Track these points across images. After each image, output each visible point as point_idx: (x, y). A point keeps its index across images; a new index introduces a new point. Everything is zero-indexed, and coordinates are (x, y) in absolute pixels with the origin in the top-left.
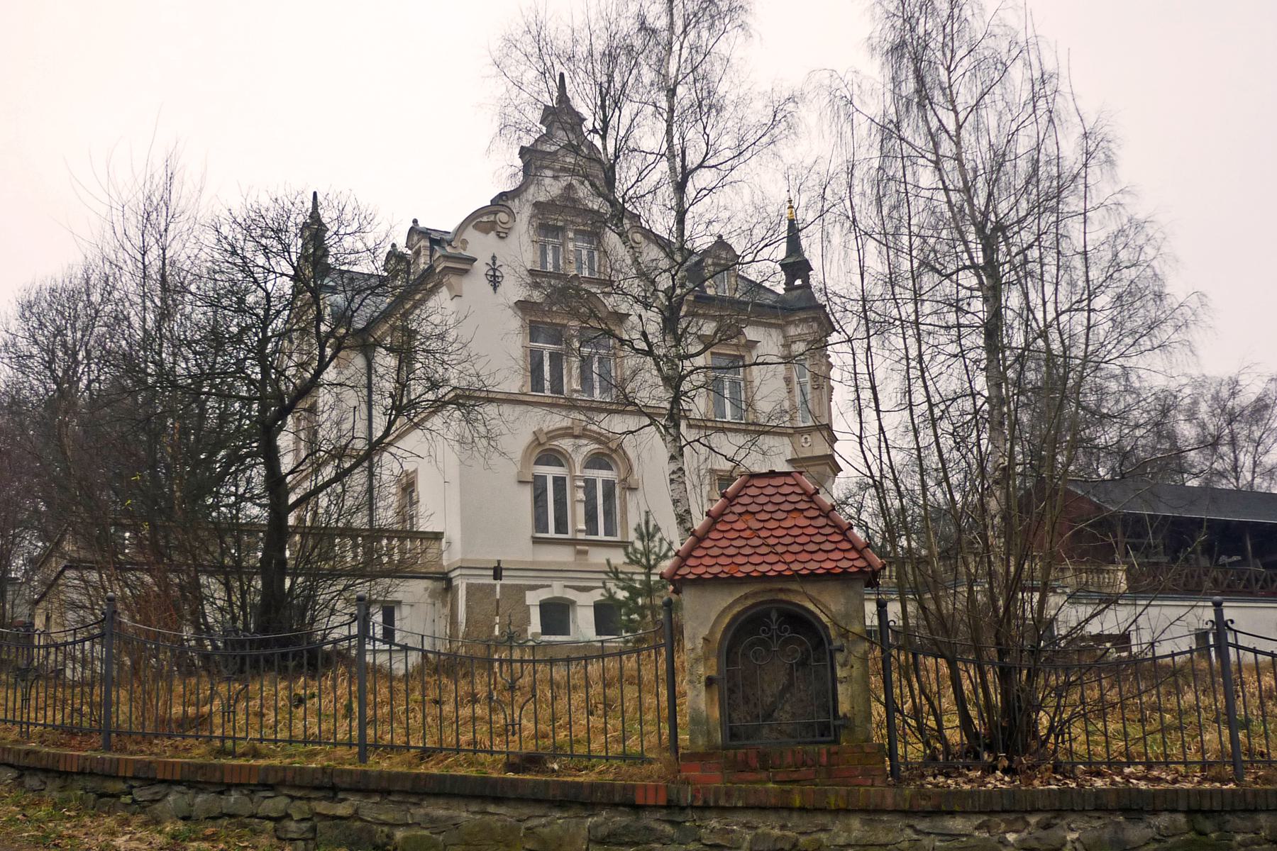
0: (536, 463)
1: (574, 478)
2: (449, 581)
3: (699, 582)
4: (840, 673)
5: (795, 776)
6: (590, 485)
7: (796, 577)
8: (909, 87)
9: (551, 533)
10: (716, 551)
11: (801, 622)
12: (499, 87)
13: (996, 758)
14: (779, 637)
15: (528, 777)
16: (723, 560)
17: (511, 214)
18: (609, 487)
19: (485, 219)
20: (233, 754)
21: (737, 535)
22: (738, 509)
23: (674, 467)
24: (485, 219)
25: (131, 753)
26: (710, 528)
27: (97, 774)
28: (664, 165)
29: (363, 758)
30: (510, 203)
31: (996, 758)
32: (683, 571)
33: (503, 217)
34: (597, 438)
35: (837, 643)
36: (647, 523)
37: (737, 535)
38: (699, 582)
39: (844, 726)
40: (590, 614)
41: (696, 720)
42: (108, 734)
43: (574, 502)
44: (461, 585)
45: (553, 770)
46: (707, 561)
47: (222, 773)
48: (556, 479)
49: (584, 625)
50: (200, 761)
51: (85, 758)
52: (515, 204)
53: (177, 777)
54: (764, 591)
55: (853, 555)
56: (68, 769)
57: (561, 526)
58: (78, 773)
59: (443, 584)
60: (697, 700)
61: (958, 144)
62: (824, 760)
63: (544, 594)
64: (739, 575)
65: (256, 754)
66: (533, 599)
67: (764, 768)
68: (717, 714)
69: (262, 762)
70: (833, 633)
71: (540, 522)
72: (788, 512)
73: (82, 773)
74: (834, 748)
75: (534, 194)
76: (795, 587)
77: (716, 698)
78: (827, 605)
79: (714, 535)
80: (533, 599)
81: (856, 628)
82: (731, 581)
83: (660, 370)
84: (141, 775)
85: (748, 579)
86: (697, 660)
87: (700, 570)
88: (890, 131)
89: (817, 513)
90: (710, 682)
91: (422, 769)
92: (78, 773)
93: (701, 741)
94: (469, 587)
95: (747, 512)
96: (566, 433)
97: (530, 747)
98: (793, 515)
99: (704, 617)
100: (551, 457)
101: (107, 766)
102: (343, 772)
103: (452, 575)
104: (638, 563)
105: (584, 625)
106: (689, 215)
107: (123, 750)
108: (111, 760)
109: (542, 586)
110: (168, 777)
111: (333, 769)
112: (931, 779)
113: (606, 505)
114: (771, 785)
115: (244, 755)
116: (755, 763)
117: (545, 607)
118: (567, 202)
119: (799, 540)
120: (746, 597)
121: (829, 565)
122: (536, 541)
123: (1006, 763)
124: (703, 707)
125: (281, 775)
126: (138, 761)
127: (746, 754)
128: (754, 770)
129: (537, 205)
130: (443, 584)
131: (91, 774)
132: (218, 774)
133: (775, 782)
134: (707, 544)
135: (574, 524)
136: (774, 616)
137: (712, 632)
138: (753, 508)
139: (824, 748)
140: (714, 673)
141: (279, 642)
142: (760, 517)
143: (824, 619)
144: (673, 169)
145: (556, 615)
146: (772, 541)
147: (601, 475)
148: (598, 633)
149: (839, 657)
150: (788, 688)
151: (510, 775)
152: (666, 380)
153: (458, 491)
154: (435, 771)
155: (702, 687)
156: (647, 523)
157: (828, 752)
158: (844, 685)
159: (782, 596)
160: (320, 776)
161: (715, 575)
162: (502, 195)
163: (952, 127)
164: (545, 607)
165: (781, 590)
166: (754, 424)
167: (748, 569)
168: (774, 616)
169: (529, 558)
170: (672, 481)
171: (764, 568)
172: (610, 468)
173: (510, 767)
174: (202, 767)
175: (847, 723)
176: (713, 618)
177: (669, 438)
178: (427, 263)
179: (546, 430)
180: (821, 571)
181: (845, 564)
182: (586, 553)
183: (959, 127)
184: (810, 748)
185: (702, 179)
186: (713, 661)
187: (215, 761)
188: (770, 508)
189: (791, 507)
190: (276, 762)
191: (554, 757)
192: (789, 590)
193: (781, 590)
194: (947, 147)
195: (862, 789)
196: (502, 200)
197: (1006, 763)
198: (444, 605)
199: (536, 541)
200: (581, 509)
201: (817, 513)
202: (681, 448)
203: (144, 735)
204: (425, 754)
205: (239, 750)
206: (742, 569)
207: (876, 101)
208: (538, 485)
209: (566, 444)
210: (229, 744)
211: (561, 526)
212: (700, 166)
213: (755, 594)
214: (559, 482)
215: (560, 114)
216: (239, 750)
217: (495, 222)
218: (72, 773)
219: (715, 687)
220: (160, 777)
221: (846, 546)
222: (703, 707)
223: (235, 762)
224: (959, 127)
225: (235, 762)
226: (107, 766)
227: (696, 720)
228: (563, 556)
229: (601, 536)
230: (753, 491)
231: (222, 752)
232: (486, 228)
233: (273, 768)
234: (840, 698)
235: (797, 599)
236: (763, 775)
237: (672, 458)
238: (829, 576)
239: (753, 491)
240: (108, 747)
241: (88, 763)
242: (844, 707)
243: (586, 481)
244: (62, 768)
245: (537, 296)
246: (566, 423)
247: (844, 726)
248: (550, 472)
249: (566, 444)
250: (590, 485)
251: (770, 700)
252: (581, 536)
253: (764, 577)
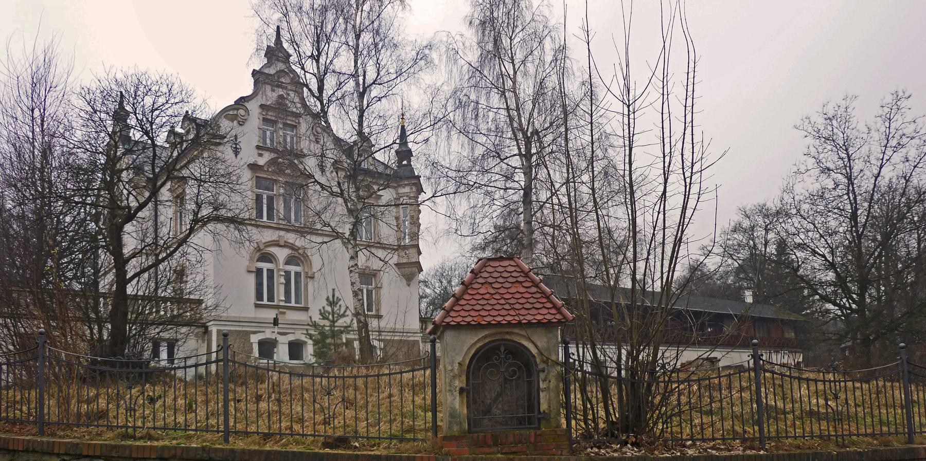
0: (257, 261)
1: (279, 270)
2: (207, 328)
3: (458, 327)
4: (542, 385)
5: (514, 450)
6: (287, 274)
7: (519, 324)
9: (265, 302)
10: (468, 308)
11: (519, 354)
13: (628, 437)
14: (505, 362)
15: (340, 452)
16: (473, 313)
17: (247, 110)
18: (298, 275)
19: (231, 113)
20: (134, 437)
21: (481, 297)
22: (481, 280)
23: (352, 263)
24: (231, 113)
25: (60, 437)
26: (464, 292)
27: (37, 452)
28: (352, 83)
29: (227, 441)
30: (246, 104)
31: (628, 437)
32: (447, 320)
33: (242, 112)
34: (292, 247)
35: (541, 366)
36: (333, 296)
37: (481, 297)
38: (458, 327)
39: (543, 418)
40: (286, 348)
41: (453, 415)
42: (42, 425)
43: (278, 284)
44: (214, 330)
45: (356, 447)
46: (463, 313)
47: (131, 450)
48: (268, 270)
49: (282, 354)
50: (112, 443)
51: (29, 441)
52: (248, 105)
53: (98, 453)
54: (496, 334)
55: (553, 311)
56: (16, 448)
57: (271, 298)
58: (23, 451)
59: (202, 330)
60: (453, 402)
61: (514, 83)
62: (532, 439)
63: (261, 336)
64: (483, 323)
65: (151, 438)
66: (255, 339)
67: (496, 444)
68: (465, 411)
69: (155, 443)
70: (538, 360)
71: (259, 296)
72: (482, 284)
73: (26, 451)
74: (538, 432)
75: (260, 100)
76: (516, 331)
77: (465, 401)
78: (533, 344)
79: (467, 297)
80: (255, 339)
81: (554, 358)
82: (480, 327)
83: (347, 205)
84: (71, 452)
85: (489, 325)
86: (454, 377)
87: (459, 319)
89: (530, 284)
90: (462, 390)
91: (267, 448)
92: (23, 451)
93: (456, 428)
94: (218, 331)
95: (517, 281)
96: (276, 244)
97: (339, 433)
98: (516, 285)
99: (457, 351)
100: (266, 257)
101: (45, 446)
102: (217, 449)
103: (208, 324)
104: (328, 319)
105: (282, 354)
106: (366, 114)
107: (53, 435)
108: (48, 442)
109: (260, 332)
110: (91, 453)
111: (210, 448)
112: (589, 450)
113: (296, 287)
114: (499, 455)
115: (141, 438)
116: (490, 442)
117: (261, 343)
118: (280, 107)
119: (520, 301)
120: (485, 337)
121: (539, 317)
122: (257, 306)
123: (634, 440)
124: (457, 406)
125: (173, 452)
126: (68, 443)
127: (485, 436)
128: (489, 446)
129: (262, 106)
130: (202, 330)
131: (34, 451)
132: (127, 452)
133: (502, 454)
134: (462, 302)
135: (278, 296)
136: (502, 349)
137: (464, 359)
138: (491, 280)
139: (532, 432)
140: (464, 385)
142: (495, 285)
143: (534, 351)
144: (357, 84)
145: (267, 347)
146: (513, 301)
147: (293, 269)
148: (290, 359)
149: (542, 376)
150: (500, 394)
151: (327, 450)
152: (350, 211)
153: (219, 272)
154: (275, 448)
155: (457, 394)
156: (333, 296)
157: (535, 434)
158: (545, 393)
159: (508, 337)
160: (201, 453)
161: (469, 322)
162: (242, 99)
163: (511, 73)
164: (261, 343)
165: (507, 333)
166: (378, 243)
167: (488, 319)
168: (502, 349)
169: (253, 316)
170: (351, 271)
171: (499, 319)
172: (298, 265)
173: (326, 445)
174: (116, 446)
175: (545, 417)
176: (465, 349)
177: (350, 246)
178: (202, 135)
179: (263, 241)
180: (534, 321)
181: (549, 317)
182: (284, 313)
183: (515, 73)
184: (523, 432)
185: (375, 91)
186: (464, 377)
187: (123, 443)
188: (501, 280)
189: (515, 280)
190: (167, 443)
191: (356, 438)
192: (512, 333)
193: (507, 333)
194: (509, 84)
195: (556, 457)
196: (241, 101)
197: (634, 440)
198: (203, 342)
199: (257, 306)
200: (282, 288)
201: (530, 284)
202: (357, 252)
203: (68, 425)
204: (267, 437)
205: (138, 435)
206: (485, 319)
207: (473, 56)
208: (259, 272)
209: (274, 250)
210: (130, 430)
211: (271, 298)
212: (374, 83)
213: (491, 335)
214: (271, 272)
215: (275, 53)
216: (138, 435)
217: (237, 115)
218: (18, 451)
219: (465, 394)
220: (85, 453)
221: (549, 305)
222: (457, 406)
223: (138, 443)
224: (515, 73)
225: (138, 443)
226: (45, 446)
227: (453, 415)
228: (271, 314)
229: (293, 304)
230: (490, 269)
231: (126, 436)
232: (233, 118)
233: (167, 447)
234: (541, 401)
235: (517, 339)
236: (495, 449)
237: (352, 258)
238: (540, 324)
239: (490, 269)
240: (42, 433)
241: (31, 444)
242: (544, 407)
243: (285, 272)
244: (11, 448)
245: (261, 161)
246: (275, 238)
247: (543, 418)
248: (265, 266)
249: (274, 250)
250: (287, 274)
251: (489, 401)
252: (282, 304)
253: (499, 324)
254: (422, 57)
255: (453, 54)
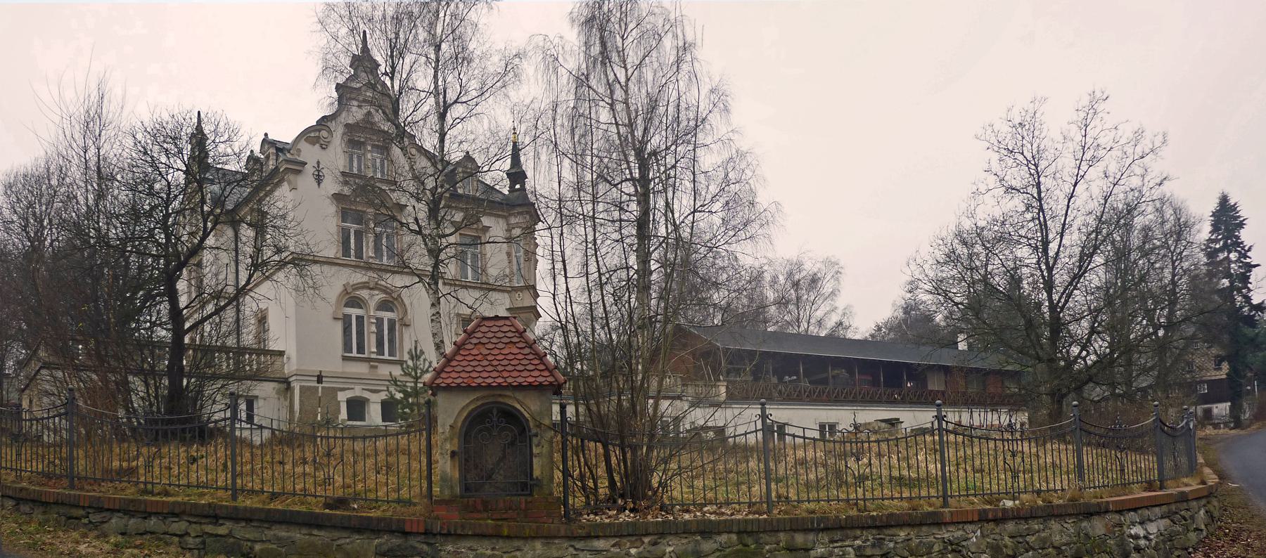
1: (369, 317)
3: (448, 388)
4: (535, 450)
6: (380, 321)
7: (510, 387)
8: (596, 50)
9: (354, 354)
11: (511, 416)
12: (323, 40)
16: (463, 375)
17: (330, 132)
18: (392, 323)
20: (152, 493)
22: (474, 341)
23: (434, 311)
26: (456, 353)
28: (432, 100)
29: (234, 498)
32: (437, 381)
33: (324, 133)
34: (385, 290)
35: (534, 431)
38: (448, 388)
40: (379, 407)
41: (444, 479)
42: (72, 478)
46: (454, 375)
48: (358, 317)
49: (374, 415)
52: (332, 125)
53: (117, 507)
55: (546, 373)
57: (361, 349)
60: (445, 466)
61: (626, 92)
62: (523, 506)
63: (349, 394)
65: (167, 494)
66: (342, 397)
67: (486, 510)
69: (171, 499)
70: (531, 424)
71: (347, 347)
73: (56, 503)
74: (530, 499)
76: (509, 393)
78: (528, 406)
80: (342, 397)
82: (469, 389)
83: (426, 244)
85: (479, 387)
88: (582, 81)
90: (453, 454)
91: (272, 506)
93: (447, 492)
96: (365, 286)
97: (340, 493)
99: (451, 411)
100: (355, 302)
102: (222, 506)
104: (410, 375)
105: (374, 415)
106: (447, 137)
107: (82, 489)
113: (390, 335)
115: (159, 494)
116: (480, 507)
118: (366, 125)
120: (477, 399)
122: (345, 358)
128: (479, 511)
129: (347, 126)
131: (62, 504)
134: (454, 363)
137: (455, 421)
139: (523, 499)
140: (456, 449)
141: (180, 421)
143: (527, 415)
144: (437, 103)
145: (357, 407)
146: (495, 363)
147: (386, 315)
148: (384, 420)
149: (535, 440)
152: (430, 251)
153: (293, 322)
154: (280, 507)
159: (501, 400)
162: (324, 118)
163: (623, 80)
167: (479, 380)
169: (340, 370)
173: (327, 506)
174: (132, 501)
175: (538, 483)
181: (541, 379)
182: (376, 367)
183: (628, 80)
185: (457, 111)
186: (456, 441)
188: (494, 340)
190: (180, 499)
191: (355, 500)
194: (619, 94)
196: (323, 121)
199: (345, 358)
200: (373, 338)
203: (95, 480)
204: (274, 496)
205: (156, 491)
207: (573, 61)
208: (346, 320)
209: (364, 293)
210: (149, 486)
211: (361, 349)
212: (456, 102)
213: (483, 397)
215: (363, 61)
216: (156, 491)
221: (542, 367)
224: (628, 80)
227: (444, 479)
228: (362, 369)
229: (386, 356)
231: (145, 492)
233: (178, 503)
234: (535, 467)
235: (510, 402)
236: (485, 515)
237: (433, 305)
239: (484, 329)
240: (72, 487)
242: (537, 473)
245: (346, 191)
246: (365, 279)
248: (354, 312)
249: (364, 293)
250: (380, 321)
252: (374, 356)
253: (489, 386)
254: (510, 70)
255: (552, 62)
